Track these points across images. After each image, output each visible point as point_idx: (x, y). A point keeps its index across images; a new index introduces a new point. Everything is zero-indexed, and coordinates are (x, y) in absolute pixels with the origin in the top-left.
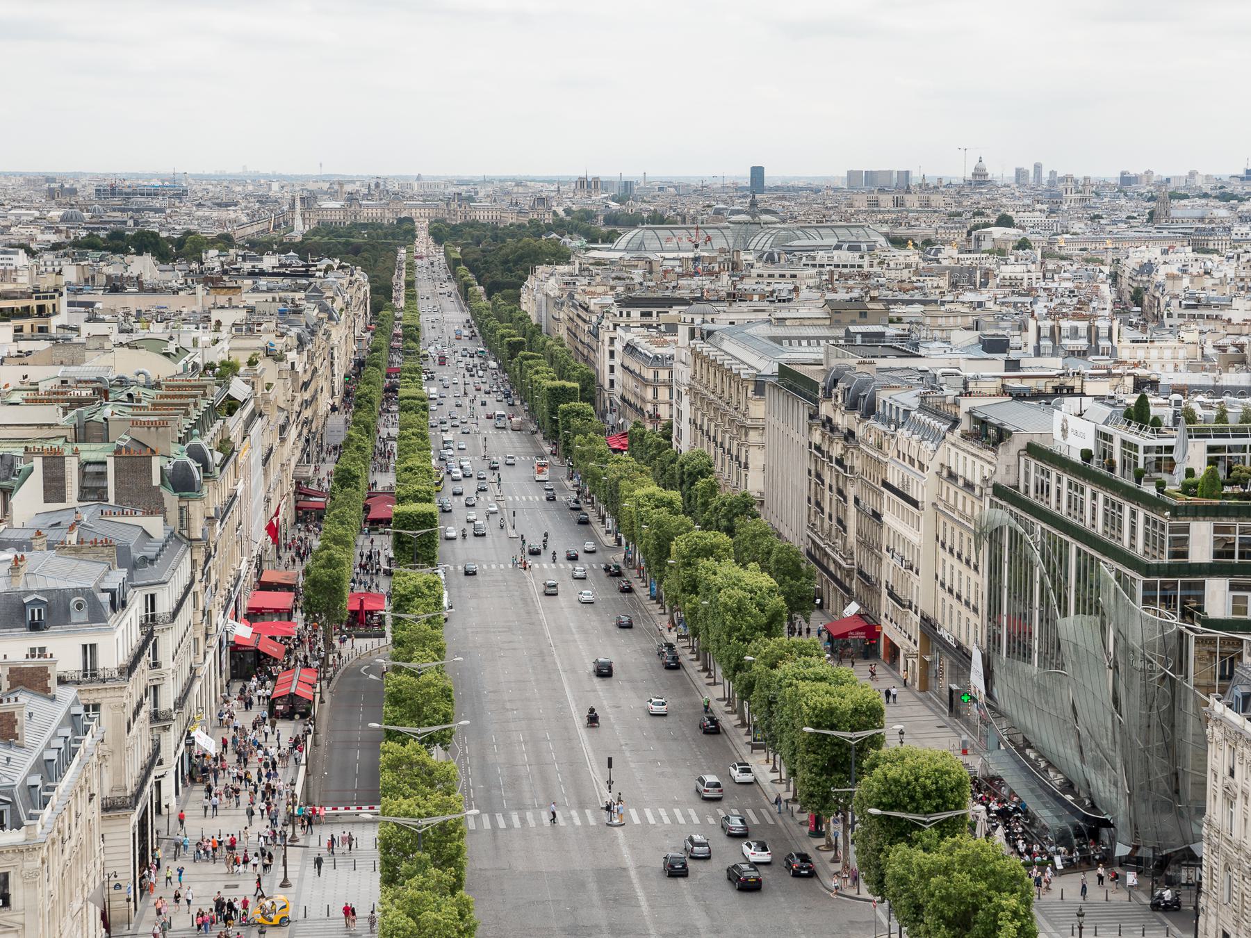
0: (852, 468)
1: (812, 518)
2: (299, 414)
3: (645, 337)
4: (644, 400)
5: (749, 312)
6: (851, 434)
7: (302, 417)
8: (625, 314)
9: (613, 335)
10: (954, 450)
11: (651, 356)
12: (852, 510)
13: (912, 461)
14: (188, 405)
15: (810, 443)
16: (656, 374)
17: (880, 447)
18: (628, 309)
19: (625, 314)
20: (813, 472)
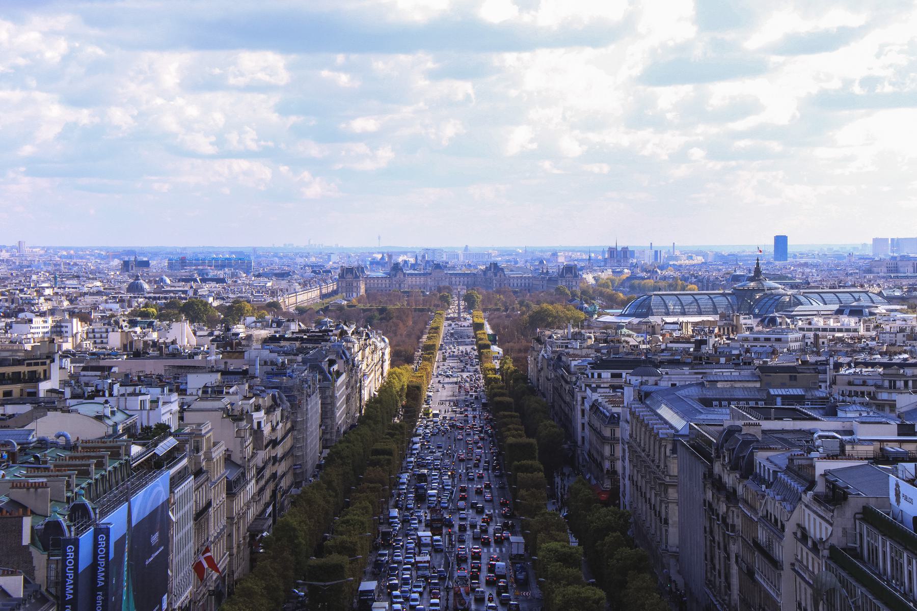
0: (733, 526)
1: (709, 574)
2: (260, 471)
3: (606, 397)
4: (602, 456)
5: (690, 374)
6: (735, 490)
7: (267, 473)
8: (596, 376)
9: (584, 394)
10: (807, 511)
11: (608, 414)
12: (734, 570)
13: (776, 520)
14: (89, 465)
15: (705, 501)
16: (613, 432)
17: (753, 509)
18: (599, 371)
19: (596, 376)
20: (708, 529)
